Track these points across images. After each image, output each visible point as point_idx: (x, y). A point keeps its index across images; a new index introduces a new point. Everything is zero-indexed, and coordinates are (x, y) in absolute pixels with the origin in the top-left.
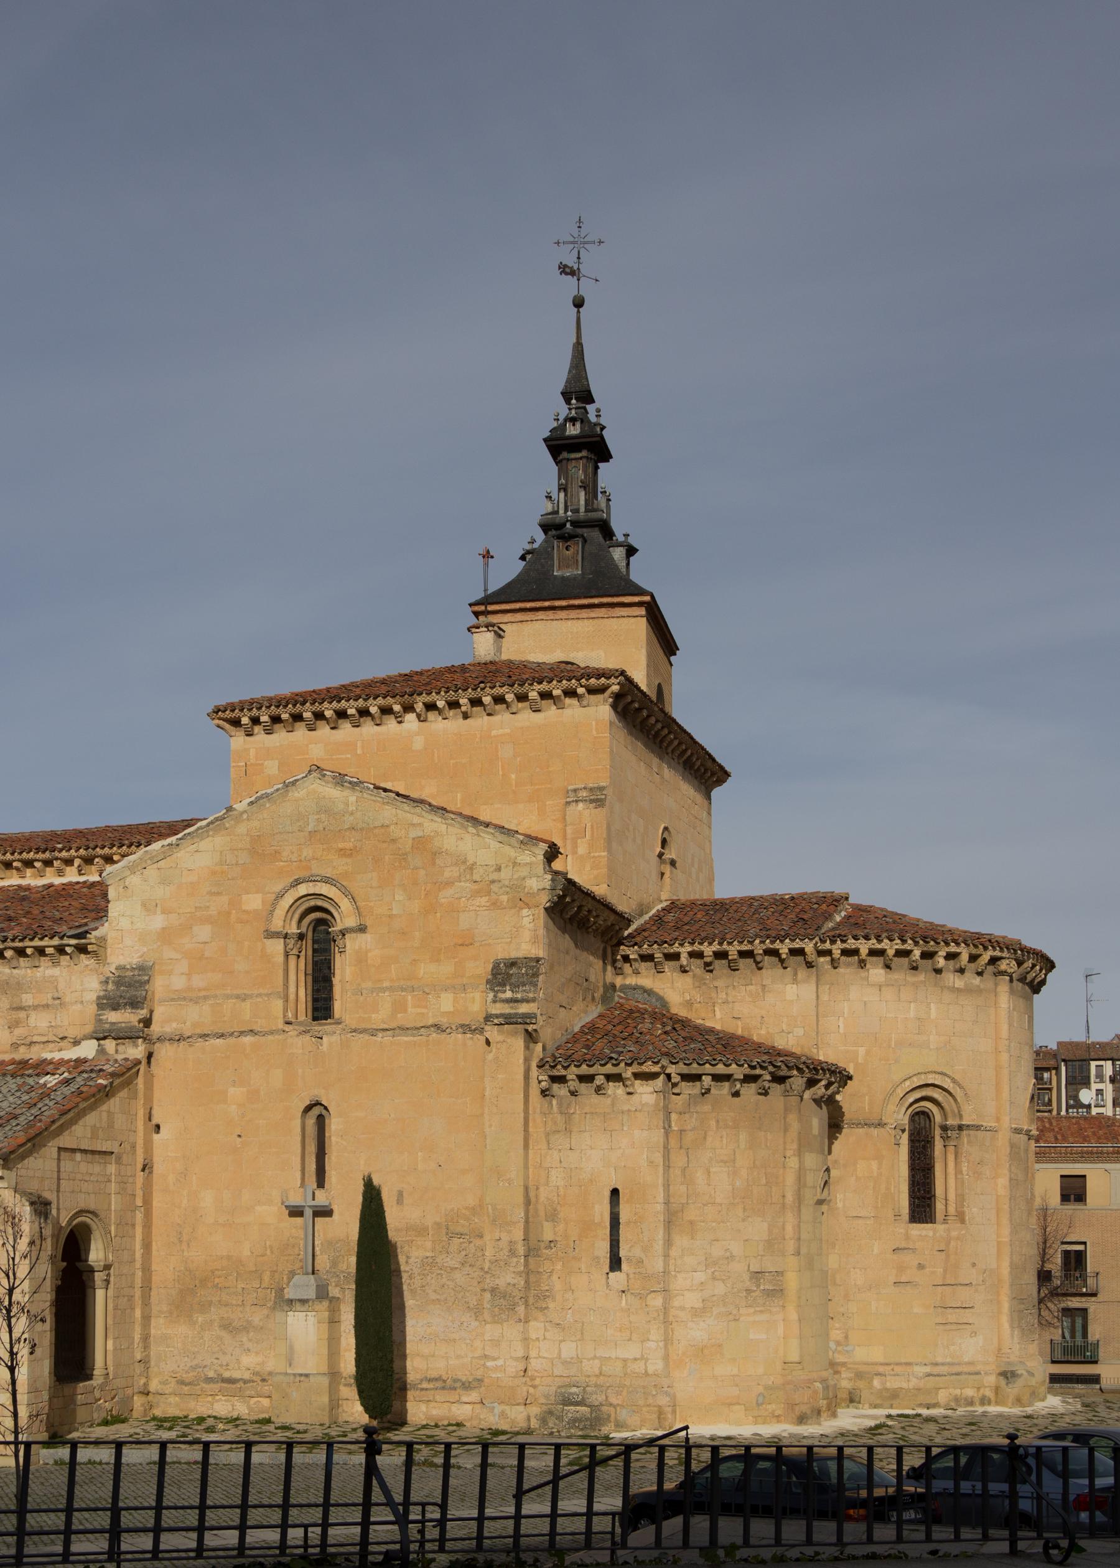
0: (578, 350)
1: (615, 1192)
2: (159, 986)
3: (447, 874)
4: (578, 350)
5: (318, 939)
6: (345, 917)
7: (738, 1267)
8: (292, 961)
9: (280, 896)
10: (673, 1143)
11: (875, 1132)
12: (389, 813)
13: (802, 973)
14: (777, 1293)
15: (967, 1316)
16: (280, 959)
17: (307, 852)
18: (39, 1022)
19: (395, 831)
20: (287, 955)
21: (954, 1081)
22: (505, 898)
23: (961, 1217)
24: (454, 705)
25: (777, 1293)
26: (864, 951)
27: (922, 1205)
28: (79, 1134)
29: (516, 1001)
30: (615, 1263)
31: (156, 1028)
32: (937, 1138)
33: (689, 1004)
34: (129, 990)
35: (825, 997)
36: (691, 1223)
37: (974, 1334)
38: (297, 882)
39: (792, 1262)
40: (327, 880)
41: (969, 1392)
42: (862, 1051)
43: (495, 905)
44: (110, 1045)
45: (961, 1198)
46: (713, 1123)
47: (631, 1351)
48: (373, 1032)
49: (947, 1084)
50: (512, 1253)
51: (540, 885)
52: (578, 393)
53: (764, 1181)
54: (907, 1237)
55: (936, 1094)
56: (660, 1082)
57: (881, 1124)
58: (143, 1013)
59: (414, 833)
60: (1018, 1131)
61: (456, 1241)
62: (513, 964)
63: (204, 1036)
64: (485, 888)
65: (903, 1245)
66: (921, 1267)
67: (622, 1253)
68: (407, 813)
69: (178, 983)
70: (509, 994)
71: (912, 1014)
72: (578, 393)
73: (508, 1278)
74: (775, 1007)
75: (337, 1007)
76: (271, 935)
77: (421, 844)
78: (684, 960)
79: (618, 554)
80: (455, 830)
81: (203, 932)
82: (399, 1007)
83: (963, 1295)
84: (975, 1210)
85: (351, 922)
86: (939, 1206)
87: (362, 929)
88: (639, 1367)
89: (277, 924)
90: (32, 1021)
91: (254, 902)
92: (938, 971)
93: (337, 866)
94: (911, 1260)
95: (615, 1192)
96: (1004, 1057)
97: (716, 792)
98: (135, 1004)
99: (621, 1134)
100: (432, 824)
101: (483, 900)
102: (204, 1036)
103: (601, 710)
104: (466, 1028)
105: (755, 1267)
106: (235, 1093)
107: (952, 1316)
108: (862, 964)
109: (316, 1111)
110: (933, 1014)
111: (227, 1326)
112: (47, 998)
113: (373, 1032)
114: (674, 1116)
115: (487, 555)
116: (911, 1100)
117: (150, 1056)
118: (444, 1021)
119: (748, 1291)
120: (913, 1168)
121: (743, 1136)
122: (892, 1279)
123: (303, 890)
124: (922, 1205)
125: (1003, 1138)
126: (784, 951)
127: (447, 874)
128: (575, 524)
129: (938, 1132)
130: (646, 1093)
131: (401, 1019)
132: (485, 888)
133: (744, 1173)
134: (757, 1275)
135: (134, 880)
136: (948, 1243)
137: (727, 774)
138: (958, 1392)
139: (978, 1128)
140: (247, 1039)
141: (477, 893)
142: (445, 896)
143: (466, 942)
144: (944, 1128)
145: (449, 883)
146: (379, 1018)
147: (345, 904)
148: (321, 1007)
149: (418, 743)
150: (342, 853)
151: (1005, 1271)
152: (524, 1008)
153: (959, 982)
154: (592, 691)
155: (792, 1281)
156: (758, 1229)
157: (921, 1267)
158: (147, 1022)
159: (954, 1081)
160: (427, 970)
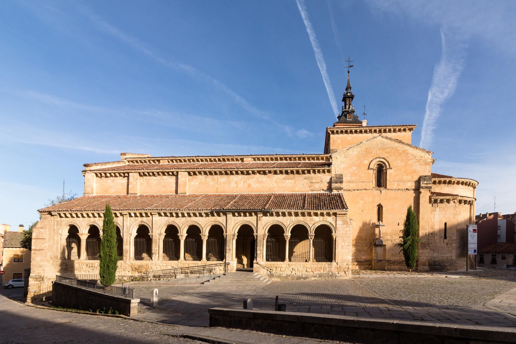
3: (410, 158)
12: (397, 145)
17: (379, 152)
18: (317, 186)
19: (399, 148)
43: (421, 164)
47: (448, 255)
64: (418, 161)
67: (447, 235)
68: (401, 145)
69: (348, 179)
77: (404, 151)
80: (412, 149)
81: (355, 168)
82: (399, 185)
88: (450, 258)
90: (315, 186)
112: (318, 181)
127: (410, 158)
131: (399, 187)
132: (418, 161)
142: (410, 162)
143: (414, 172)
145: (411, 160)
146: (394, 187)
150: (386, 152)
160: (405, 177)
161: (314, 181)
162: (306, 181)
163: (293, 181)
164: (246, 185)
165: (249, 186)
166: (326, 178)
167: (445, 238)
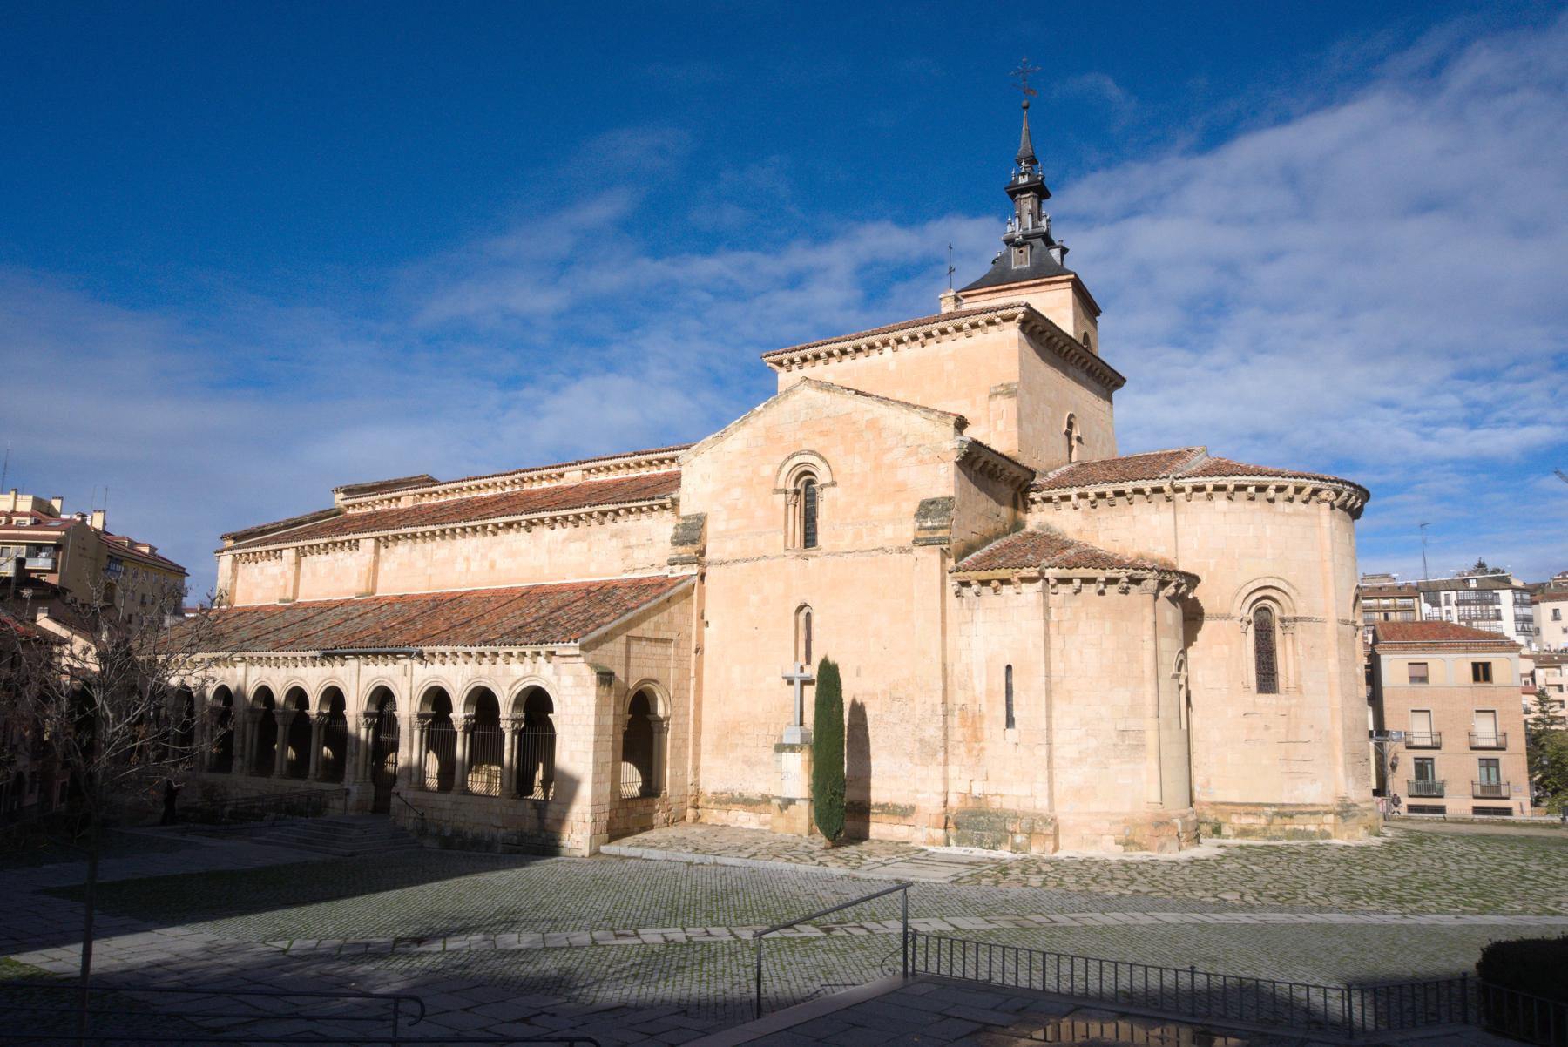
1: (1009, 668)
2: (711, 529)
5: (806, 493)
6: (822, 476)
8: (791, 508)
9: (782, 466)
10: (1052, 630)
11: (1225, 623)
13: (1164, 505)
15: (1306, 767)
16: (783, 507)
17: (800, 435)
18: (639, 555)
20: (787, 505)
21: (1288, 584)
22: (927, 457)
23: (1299, 689)
24: (914, 338)
25: (1139, 747)
26: (1210, 487)
27: (1267, 679)
28: (646, 629)
29: (935, 528)
30: (1010, 722)
31: (708, 557)
32: (1278, 629)
33: (1080, 531)
34: (691, 534)
35: (1180, 523)
36: (1069, 692)
37: (1314, 781)
38: (794, 455)
40: (812, 452)
41: (1311, 828)
42: (1212, 562)
43: (921, 461)
44: (677, 568)
45: (1299, 674)
46: (1083, 615)
48: (841, 555)
49: (1282, 585)
50: (934, 712)
51: (951, 445)
54: (1255, 704)
55: (1274, 594)
56: (1040, 584)
57: (1229, 617)
58: (698, 547)
59: (868, 416)
60: (1345, 622)
61: (897, 703)
62: (933, 502)
63: (736, 561)
66: (1267, 728)
67: (1016, 714)
69: (721, 526)
70: (929, 524)
73: (933, 732)
74: (1137, 529)
75: (820, 538)
76: (777, 491)
77: (873, 424)
78: (1074, 497)
79: (1055, 253)
85: (827, 480)
86: (1281, 681)
87: (834, 484)
89: (781, 485)
91: (767, 470)
92: (1271, 501)
93: (817, 443)
95: (1009, 668)
96: (1329, 565)
97: (1116, 394)
98: (693, 542)
99: (1008, 621)
100: (879, 409)
101: (913, 459)
102: (736, 561)
103: (1012, 331)
104: (903, 550)
105: (1121, 727)
106: (754, 598)
107: (1295, 767)
108: (1210, 497)
109: (805, 610)
110: (1268, 532)
111: (747, 762)
113: (841, 555)
114: (1053, 610)
117: (702, 577)
118: (887, 546)
120: (1258, 651)
121: (1108, 625)
123: (797, 460)
124: (1267, 679)
125: (1331, 628)
126: (1148, 490)
128: (1026, 237)
129: (1278, 623)
130: (1031, 591)
132: (913, 451)
135: (696, 461)
137: (1124, 380)
139: (1310, 619)
140: (762, 562)
141: (909, 454)
142: (888, 458)
143: (901, 488)
144: (1283, 620)
145: (890, 449)
146: (844, 545)
147: (823, 467)
148: (810, 539)
149: (892, 366)
150: (822, 433)
151: (1338, 732)
152: (940, 534)
153: (1288, 508)
154: (1006, 319)
157: (1267, 728)
158: (702, 553)
159: (1288, 584)
161: (633, 541)
162: (614, 541)
163: (585, 545)
164: (486, 564)
165: (492, 565)
166: (661, 527)
167: (1010, 722)
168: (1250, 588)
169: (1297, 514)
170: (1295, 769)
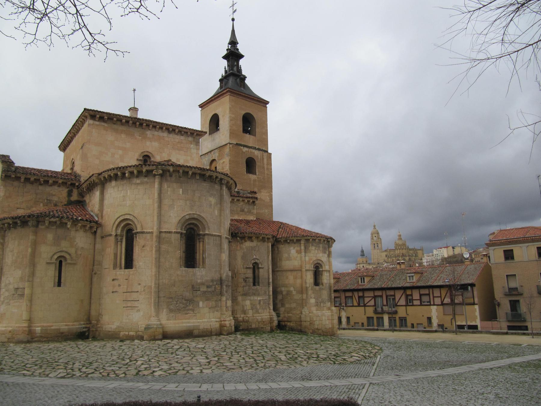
0: (233, 31)
4: (233, 31)
7: (11, 287)
14: (22, 295)
15: (136, 304)
25: (22, 295)
27: (129, 264)
39: (27, 284)
42: (109, 210)
46: (10, 239)
52: (233, 42)
53: (21, 257)
65: (115, 278)
71: (122, 195)
72: (233, 42)
83: (135, 296)
84: (141, 263)
94: (116, 282)
105: (16, 287)
110: (128, 194)
115: (134, 90)
116: (122, 225)
119: (13, 295)
121: (16, 242)
122: (111, 291)
133: (15, 254)
134: (16, 289)
136: (129, 276)
138: (127, 333)
139: (143, 233)
151: (153, 285)
155: (27, 291)
156: (18, 273)
157: (119, 285)
159: (134, 216)
168: (119, 220)
169: (142, 183)
170: (129, 305)
